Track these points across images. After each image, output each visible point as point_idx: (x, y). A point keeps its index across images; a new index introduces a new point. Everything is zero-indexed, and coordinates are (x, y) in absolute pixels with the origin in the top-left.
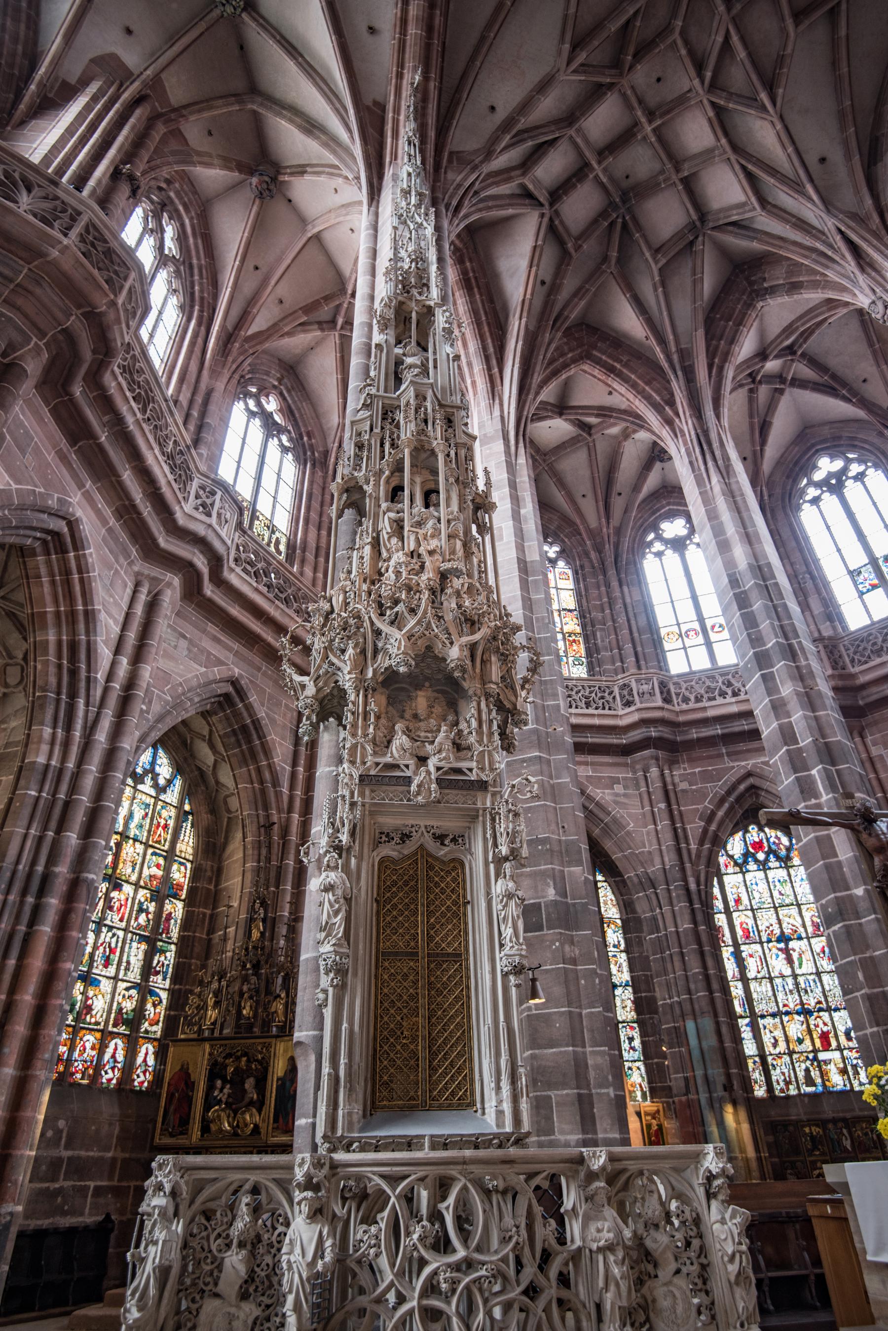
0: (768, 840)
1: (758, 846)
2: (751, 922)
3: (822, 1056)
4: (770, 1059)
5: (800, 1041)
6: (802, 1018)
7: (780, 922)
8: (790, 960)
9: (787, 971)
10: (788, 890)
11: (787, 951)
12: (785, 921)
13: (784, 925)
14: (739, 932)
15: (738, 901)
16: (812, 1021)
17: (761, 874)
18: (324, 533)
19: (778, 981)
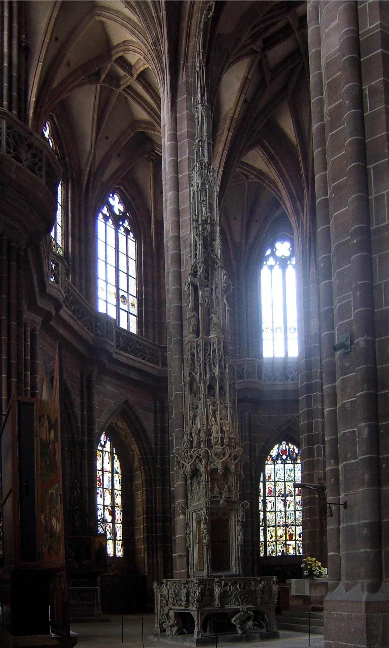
0: (289, 449)
1: (284, 452)
2: (273, 487)
3: (288, 543)
4: (268, 543)
5: (281, 537)
6: (284, 528)
7: (285, 488)
8: (285, 505)
9: (283, 509)
10: (292, 474)
11: (285, 501)
12: (287, 487)
13: (287, 490)
14: (267, 491)
15: (270, 477)
16: (288, 530)
17: (282, 465)
18: (83, 246)
19: (278, 513)
